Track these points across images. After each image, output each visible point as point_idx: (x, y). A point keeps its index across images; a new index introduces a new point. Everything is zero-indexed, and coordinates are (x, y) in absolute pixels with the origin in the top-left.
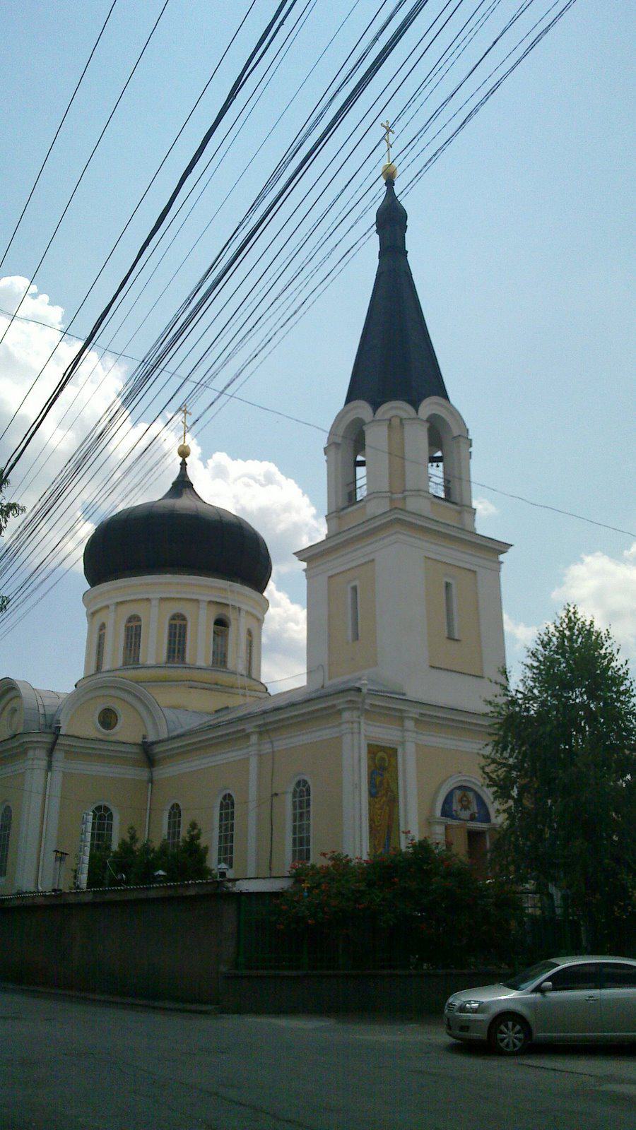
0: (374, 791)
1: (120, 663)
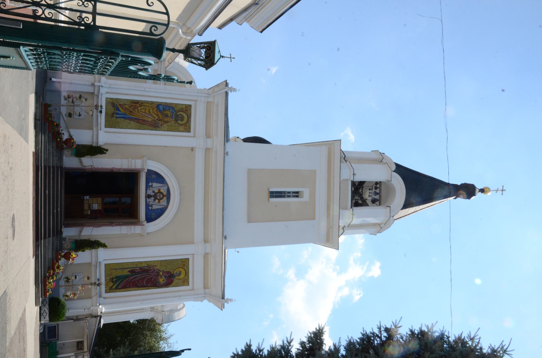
0: (161, 108)
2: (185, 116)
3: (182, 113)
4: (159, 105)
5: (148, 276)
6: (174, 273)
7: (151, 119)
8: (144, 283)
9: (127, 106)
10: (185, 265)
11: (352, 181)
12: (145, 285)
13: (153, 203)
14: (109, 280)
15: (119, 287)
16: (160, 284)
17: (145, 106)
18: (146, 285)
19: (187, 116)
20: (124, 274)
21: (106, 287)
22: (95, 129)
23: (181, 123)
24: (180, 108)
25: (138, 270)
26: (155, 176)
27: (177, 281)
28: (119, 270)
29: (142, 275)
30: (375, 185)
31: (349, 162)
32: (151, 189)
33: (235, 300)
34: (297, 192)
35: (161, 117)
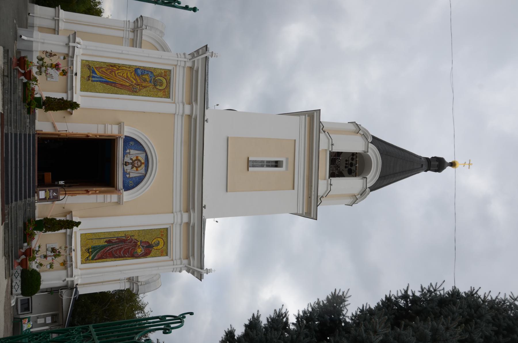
0: (139, 72)
2: (164, 81)
3: (161, 78)
4: (137, 69)
5: (125, 247)
6: (152, 243)
7: (129, 83)
8: (122, 253)
9: (103, 69)
10: (163, 234)
11: (330, 151)
12: (123, 256)
13: (131, 171)
14: (85, 250)
15: (95, 258)
16: (138, 255)
17: (122, 70)
18: (123, 255)
19: (166, 81)
20: (100, 244)
21: (81, 258)
22: (69, 92)
23: (161, 88)
24: (159, 73)
25: (115, 240)
26: (133, 143)
27: (155, 251)
28: (95, 240)
29: (119, 245)
30: (351, 157)
31: (328, 132)
32: (128, 156)
33: (214, 271)
34: (277, 162)
35: (139, 81)
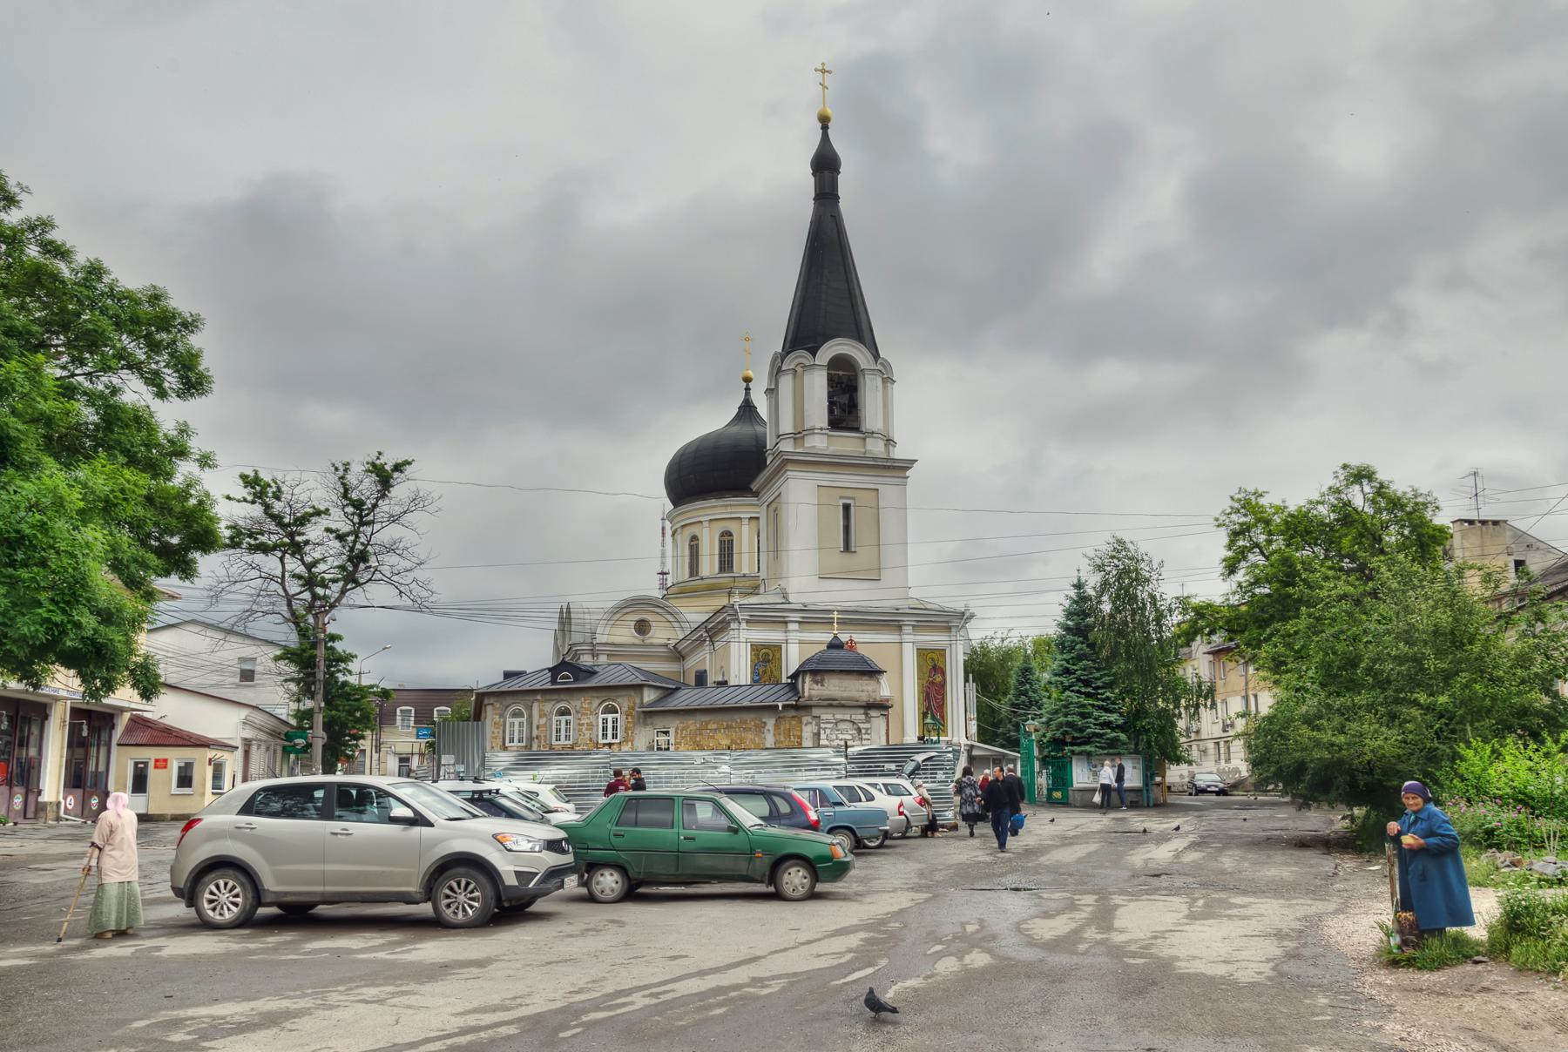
0: (756, 678)
1: (717, 570)
2: (763, 651)
